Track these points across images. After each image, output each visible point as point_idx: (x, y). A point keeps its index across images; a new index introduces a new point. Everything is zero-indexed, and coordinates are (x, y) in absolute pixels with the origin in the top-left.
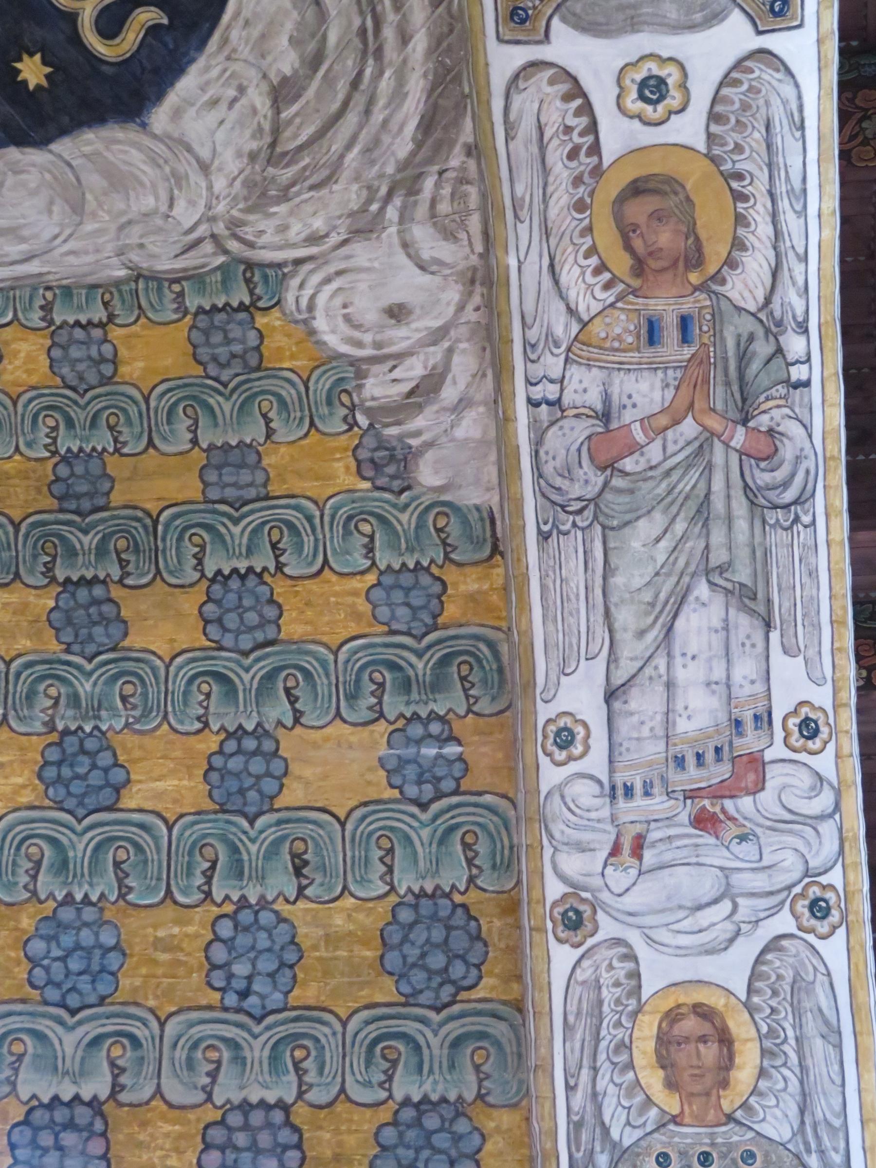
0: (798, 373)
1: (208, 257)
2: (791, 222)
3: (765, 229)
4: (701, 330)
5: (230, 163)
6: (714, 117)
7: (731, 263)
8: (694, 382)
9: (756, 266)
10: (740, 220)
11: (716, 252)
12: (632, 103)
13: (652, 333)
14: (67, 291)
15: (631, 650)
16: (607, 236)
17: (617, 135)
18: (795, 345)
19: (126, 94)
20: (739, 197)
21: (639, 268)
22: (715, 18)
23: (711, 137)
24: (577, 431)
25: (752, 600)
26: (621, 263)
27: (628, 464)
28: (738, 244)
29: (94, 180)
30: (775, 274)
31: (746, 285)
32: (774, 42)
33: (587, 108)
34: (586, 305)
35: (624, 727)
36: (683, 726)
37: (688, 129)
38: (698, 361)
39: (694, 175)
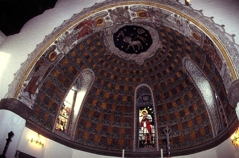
0: (152, 8)
1: (157, 30)
2: (141, 7)
3: (142, 9)
4: (150, 13)
5: (150, 27)
6: (135, 11)
7: (144, 11)
8: (154, 15)
9: (145, 9)
10: (141, 10)
11: (144, 12)
12: (134, 16)
13: (150, 16)
14: (160, 37)
15: (171, 24)
16: (143, 18)
17: (137, 17)
18: (150, 7)
19: (147, 32)
20: (140, 10)
21: (146, 16)
22: (128, 11)
23: (136, 11)
24: (157, 22)
25: (167, 16)
26: (145, 17)
27: (159, 20)
28: (143, 10)
29: (153, 34)
30: (145, 8)
31: (146, 10)
32: (129, 8)
33: (135, 18)
34: (149, 20)
35: (176, 27)
36: (176, 24)
37: (136, 13)
38: (151, 14)
39: (139, 12)
